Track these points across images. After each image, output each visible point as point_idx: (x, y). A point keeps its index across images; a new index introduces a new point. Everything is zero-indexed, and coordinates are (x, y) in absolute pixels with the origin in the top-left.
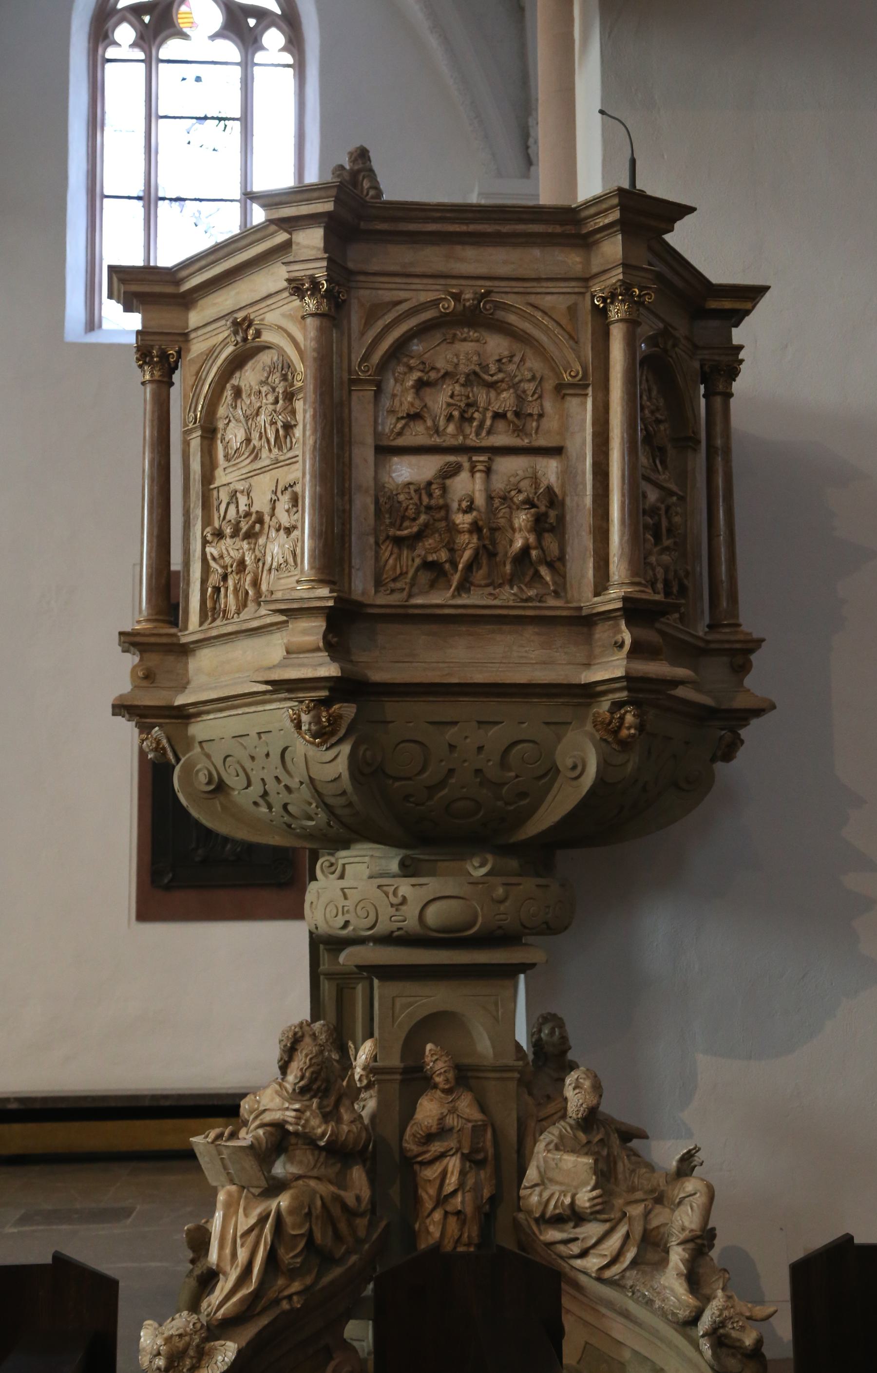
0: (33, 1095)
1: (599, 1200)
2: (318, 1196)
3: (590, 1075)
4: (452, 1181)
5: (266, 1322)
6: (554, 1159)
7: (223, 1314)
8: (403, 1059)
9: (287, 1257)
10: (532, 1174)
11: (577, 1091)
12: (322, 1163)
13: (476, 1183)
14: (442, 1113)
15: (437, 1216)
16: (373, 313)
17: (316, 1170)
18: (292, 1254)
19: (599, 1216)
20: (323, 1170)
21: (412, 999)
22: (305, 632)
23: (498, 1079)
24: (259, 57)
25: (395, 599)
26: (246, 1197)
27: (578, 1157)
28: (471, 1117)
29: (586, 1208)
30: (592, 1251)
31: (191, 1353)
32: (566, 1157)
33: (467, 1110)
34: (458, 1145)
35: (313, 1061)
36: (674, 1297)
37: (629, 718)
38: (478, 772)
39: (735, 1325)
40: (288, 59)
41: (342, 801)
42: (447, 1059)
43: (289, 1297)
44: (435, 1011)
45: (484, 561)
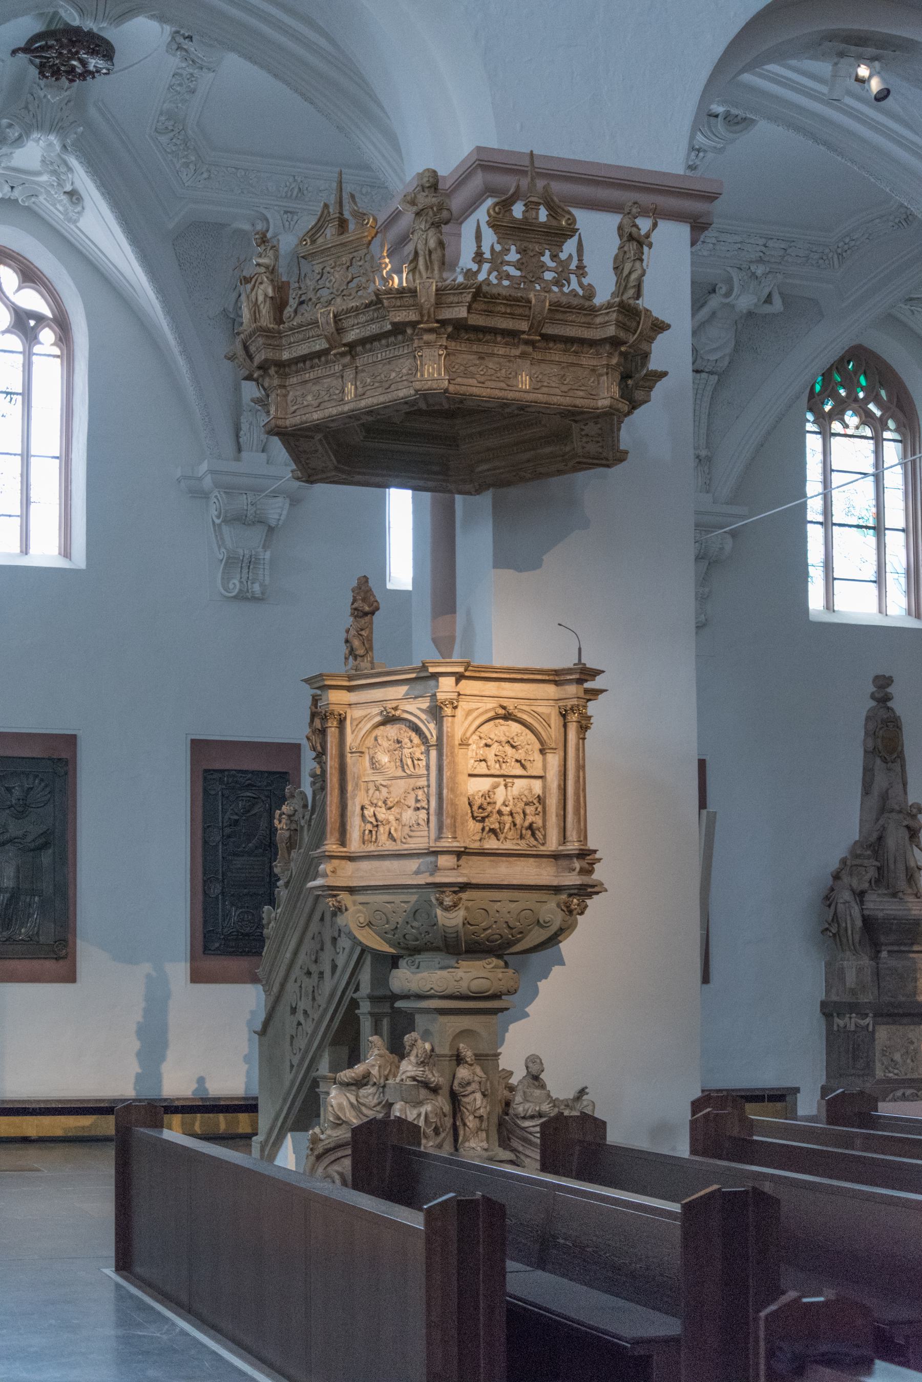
16: (469, 713)
22: (446, 861)
24: (37, 349)
25: (476, 845)
37: (575, 900)
38: (507, 922)
40: (57, 351)
41: (454, 935)
45: (512, 828)
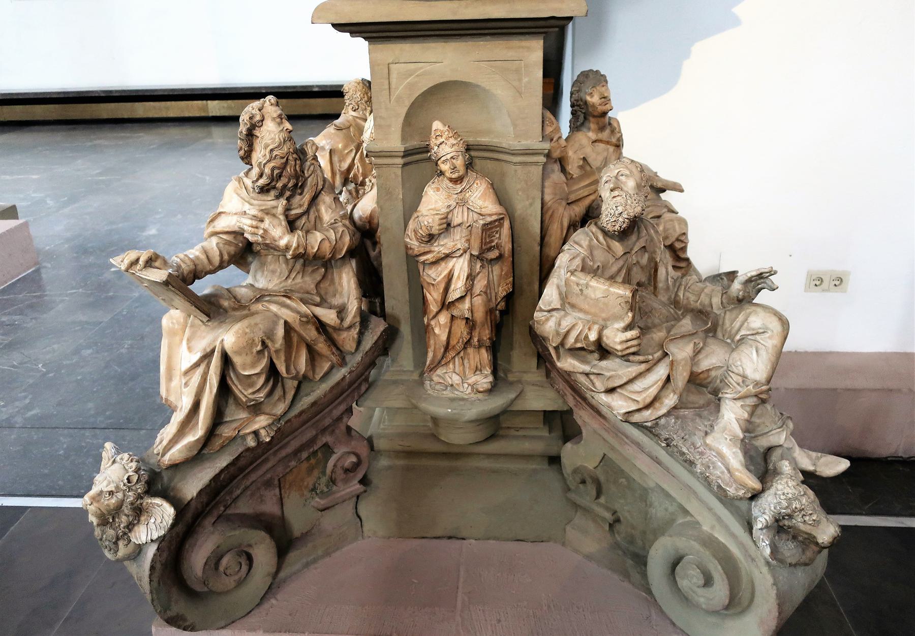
0: (326, 84)
1: (634, 342)
2: (282, 322)
3: (634, 170)
4: (458, 288)
5: (224, 464)
6: (578, 284)
7: (169, 460)
8: (404, 139)
9: (243, 392)
10: (550, 294)
11: (616, 193)
12: (298, 272)
13: (488, 286)
14: (450, 206)
15: (443, 318)
17: (290, 281)
18: (250, 391)
19: (631, 358)
20: (299, 279)
21: (412, 66)
23: (521, 163)
26: (192, 326)
27: (611, 286)
28: (484, 211)
29: (618, 351)
30: (619, 390)
31: (126, 509)
32: (593, 283)
33: (480, 203)
34: (467, 245)
35: (275, 153)
36: (722, 463)
39: (807, 518)
42: (455, 142)
43: (256, 433)
44: (442, 81)
